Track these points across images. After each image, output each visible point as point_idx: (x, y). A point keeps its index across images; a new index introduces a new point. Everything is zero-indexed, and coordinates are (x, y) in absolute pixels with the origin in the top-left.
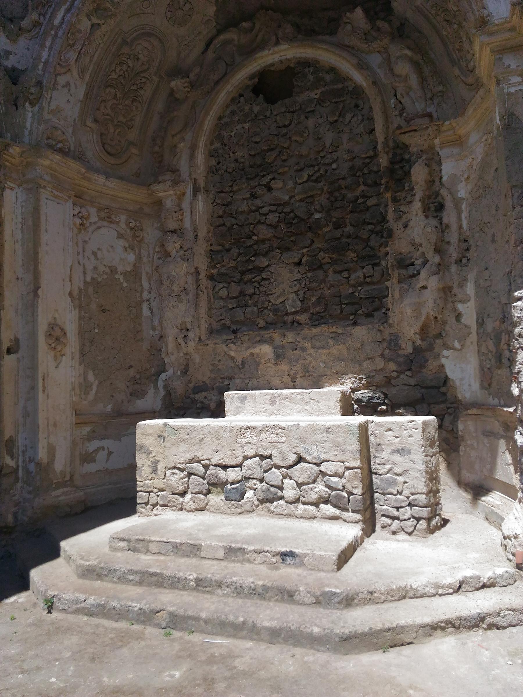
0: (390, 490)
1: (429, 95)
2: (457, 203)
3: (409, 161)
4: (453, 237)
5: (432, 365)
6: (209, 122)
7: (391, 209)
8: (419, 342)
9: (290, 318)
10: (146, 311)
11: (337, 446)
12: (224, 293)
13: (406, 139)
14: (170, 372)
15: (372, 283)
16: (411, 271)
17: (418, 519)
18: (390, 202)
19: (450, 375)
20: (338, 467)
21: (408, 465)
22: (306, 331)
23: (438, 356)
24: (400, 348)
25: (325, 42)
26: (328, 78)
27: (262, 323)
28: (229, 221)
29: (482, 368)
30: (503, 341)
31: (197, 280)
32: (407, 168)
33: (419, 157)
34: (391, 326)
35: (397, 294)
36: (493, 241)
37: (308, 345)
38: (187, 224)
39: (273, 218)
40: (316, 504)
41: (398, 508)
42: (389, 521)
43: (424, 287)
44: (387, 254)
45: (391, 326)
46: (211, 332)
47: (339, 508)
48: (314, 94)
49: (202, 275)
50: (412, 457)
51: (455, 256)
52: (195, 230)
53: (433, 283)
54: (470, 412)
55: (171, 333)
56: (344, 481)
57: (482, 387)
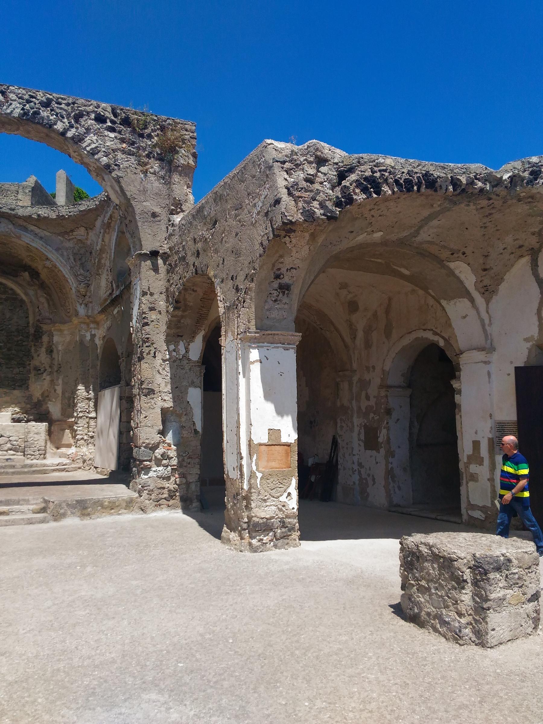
0: (32, 446)
1: (51, 312)
2: (58, 351)
3: (42, 332)
4: (56, 363)
5: (44, 407)
8: (40, 398)
11: (17, 431)
13: (41, 325)
15: (23, 374)
16: (39, 372)
17: (41, 455)
18: (33, 346)
19: (50, 410)
20: (17, 438)
21: (39, 438)
23: (47, 403)
24: (32, 400)
25: (12, 280)
26: (10, 292)
29: (62, 408)
30: (71, 400)
32: (41, 335)
33: (46, 333)
34: (29, 391)
35: (33, 380)
36: (71, 368)
40: (7, 451)
41: (34, 452)
42: (30, 456)
43: (45, 379)
44: (30, 364)
45: (29, 391)
47: (15, 451)
50: (41, 435)
51: (56, 369)
53: (48, 378)
54: (56, 423)
56: (18, 442)
57: (62, 415)
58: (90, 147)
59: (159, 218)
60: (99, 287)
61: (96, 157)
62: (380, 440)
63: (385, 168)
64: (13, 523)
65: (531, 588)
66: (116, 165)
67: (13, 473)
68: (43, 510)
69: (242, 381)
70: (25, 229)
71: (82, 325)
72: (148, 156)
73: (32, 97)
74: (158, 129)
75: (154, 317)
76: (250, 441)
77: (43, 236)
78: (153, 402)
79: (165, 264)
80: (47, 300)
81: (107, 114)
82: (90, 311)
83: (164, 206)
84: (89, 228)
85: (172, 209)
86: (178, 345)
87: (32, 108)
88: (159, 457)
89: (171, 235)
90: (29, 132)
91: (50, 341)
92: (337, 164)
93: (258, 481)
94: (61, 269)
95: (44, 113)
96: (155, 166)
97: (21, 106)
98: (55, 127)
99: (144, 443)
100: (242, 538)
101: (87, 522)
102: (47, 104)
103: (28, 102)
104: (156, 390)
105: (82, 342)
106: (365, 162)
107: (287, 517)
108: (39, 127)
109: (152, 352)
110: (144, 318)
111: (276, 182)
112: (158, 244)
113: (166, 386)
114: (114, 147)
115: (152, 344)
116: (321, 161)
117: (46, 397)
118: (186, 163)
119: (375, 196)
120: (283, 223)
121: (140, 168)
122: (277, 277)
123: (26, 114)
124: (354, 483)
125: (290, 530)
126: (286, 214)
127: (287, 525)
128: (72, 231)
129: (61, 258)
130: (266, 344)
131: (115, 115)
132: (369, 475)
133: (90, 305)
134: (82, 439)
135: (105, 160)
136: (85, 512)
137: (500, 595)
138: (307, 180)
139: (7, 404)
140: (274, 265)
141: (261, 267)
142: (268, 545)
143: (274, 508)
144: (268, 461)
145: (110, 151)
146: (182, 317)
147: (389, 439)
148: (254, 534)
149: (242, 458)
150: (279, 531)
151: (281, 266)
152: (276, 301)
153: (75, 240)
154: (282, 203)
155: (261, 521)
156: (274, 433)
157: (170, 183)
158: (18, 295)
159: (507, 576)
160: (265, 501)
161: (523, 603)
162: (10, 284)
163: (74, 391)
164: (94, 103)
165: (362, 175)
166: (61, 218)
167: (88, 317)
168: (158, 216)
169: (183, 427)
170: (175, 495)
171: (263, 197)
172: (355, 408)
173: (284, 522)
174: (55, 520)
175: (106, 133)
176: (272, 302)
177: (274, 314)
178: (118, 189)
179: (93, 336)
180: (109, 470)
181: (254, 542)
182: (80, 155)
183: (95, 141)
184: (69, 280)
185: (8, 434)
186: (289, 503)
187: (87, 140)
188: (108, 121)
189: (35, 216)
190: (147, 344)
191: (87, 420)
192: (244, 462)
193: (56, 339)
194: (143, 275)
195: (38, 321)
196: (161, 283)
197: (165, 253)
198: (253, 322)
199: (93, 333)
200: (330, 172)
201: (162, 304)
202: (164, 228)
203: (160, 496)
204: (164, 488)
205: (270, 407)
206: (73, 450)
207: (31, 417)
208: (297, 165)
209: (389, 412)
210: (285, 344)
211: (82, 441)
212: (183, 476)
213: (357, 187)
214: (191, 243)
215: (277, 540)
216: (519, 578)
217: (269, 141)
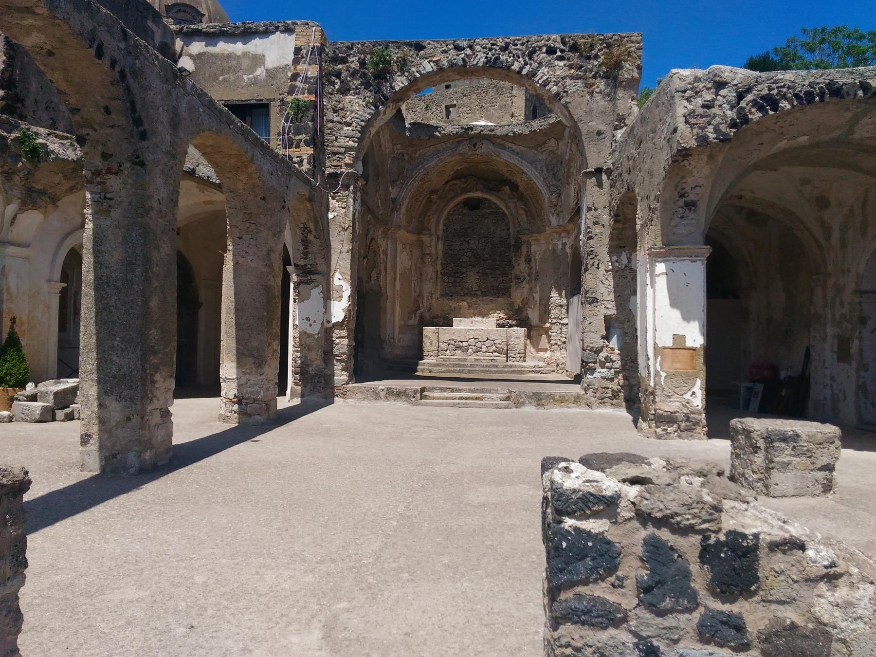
4: (534, 271)
5: (524, 313)
6: (446, 212)
7: (514, 259)
9: (473, 293)
10: (413, 285)
11: (500, 335)
12: (447, 280)
13: (521, 236)
14: (422, 310)
16: (519, 281)
22: (480, 298)
23: (526, 310)
27: (462, 294)
28: (450, 252)
29: (540, 315)
31: (437, 275)
37: (481, 303)
38: (433, 251)
39: (469, 254)
46: (441, 296)
48: (488, 211)
49: (439, 273)
52: (437, 254)
53: (527, 286)
55: (426, 294)
58: (542, 80)
59: (604, 136)
60: (569, 196)
61: (547, 88)
62: (852, 351)
63: (783, 84)
64: (485, 406)
65: (822, 460)
66: (565, 92)
67: (496, 372)
68: (508, 398)
69: (649, 291)
70: (504, 147)
71: (555, 235)
72: (594, 77)
73: (493, 44)
74: (604, 47)
75: (597, 231)
76: (655, 344)
77: (519, 151)
78: (596, 309)
79: (609, 179)
80: (525, 211)
81: (557, 45)
82: (561, 220)
83: (608, 122)
84: (559, 139)
85: (617, 125)
86: (620, 256)
87: (493, 55)
88: (603, 359)
89: (614, 151)
90: (493, 75)
91: (529, 251)
92: (736, 85)
93: (662, 379)
94: (535, 181)
95: (503, 58)
96: (601, 84)
97: (485, 55)
98: (513, 67)
99: (589, 346)
100: (650, 427)
101: (541, 411)
102: (505, 49)
103: (491, 50)
104: (600, 298)
105: (554, 251)
106: (763, 81)
107: (692, 412)
108: (499, 70)
109: (596, 264)
110: (588, 233)
111: (675, 111)
112: (603, 161)
113: (609, 295)
114: (563, 75)
115: (596, 256)
116: (720, 85)
117: (525, 303)
118: (630, 77)
119: (771, 113)
120: (678, 150)
121: (586, 90)
122: (682, 196)
123: (488, 61)
124: (825, 398)
125: (694, 425)
126: (681, 142)
127: (691, 420)
128: (545, 143)
129: (535, 171)
130: (672, 258)
131: (564, 44)
132: (840, 390)
133: (562, 214)
134: (556, 344)
135: (555, 89)
136: (540, 402)
137: (787, 459)
138: (703, 106)
139: (495, 310)
140: (677, 186)
141: (664, 189)
142: (672, 435)
143: (677, 404)
144: (672, 363)
145: (560, 79)
146: (623, 229)
147: (861, 351)
148: (659, 424)
149: (649, 359)
150: (684, 424)
151: (684, 185)
152: (682, 217)
153: (547, 152)
154: (679, 132)
155: (665, 414)
156: (679, 339)
157: (614, 99)
158: (500, 208)
159: (794, 447)
160: (669, 397)
161: (812, 470)
162: (494, 199)
163: (549, 297)
164: (545, 37)
165: (758, 95)
166: (533, 132)
167: (559, 226)
168: (603, 133)
169: (625, 333)
170: (619, 395)
171: (667, 124)
172: (829, 316)
173: (688, 417)
174: (516, 407)
175: (556, 63)
176: (678, 219)
177: (681, 230)
178: (567, 113)
179: (564, 245)
180: (575, 373)
181: (659, 430)
182: (534, 88)
183: (546, 73)
184: (543, 192)
185: (493, 337)
186: (693, 400)
187: (540, 74)
188: (558, 50)
189: (511, 134)
190: (591, 257)
191: (560, 326)
192: (651, 363)
193: (533, 248)
194: (587, 193)
195: (518, 232)
196: (605, 197)
197: (608, 169)
198: (660, 238)
199: (564, 242)
200: (729, 94)
201: (606, 218)
202: (609, 145)
203: (604, 395)
204: (608, 388)
205: (676, 314)
206: (548, 354)
207: (514, 322)
208: (697, 93)
209: (863, 321)
210: (692, 257)
211: (556, 346)
212: (626, 378)
213: (753, 106)
214: (625, 160)
215: (681, 431)
216: (808, 450)
217: (674, 71)
